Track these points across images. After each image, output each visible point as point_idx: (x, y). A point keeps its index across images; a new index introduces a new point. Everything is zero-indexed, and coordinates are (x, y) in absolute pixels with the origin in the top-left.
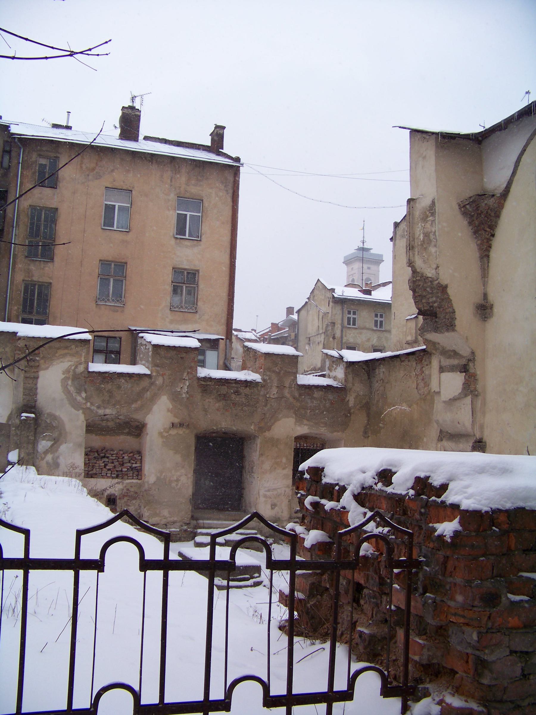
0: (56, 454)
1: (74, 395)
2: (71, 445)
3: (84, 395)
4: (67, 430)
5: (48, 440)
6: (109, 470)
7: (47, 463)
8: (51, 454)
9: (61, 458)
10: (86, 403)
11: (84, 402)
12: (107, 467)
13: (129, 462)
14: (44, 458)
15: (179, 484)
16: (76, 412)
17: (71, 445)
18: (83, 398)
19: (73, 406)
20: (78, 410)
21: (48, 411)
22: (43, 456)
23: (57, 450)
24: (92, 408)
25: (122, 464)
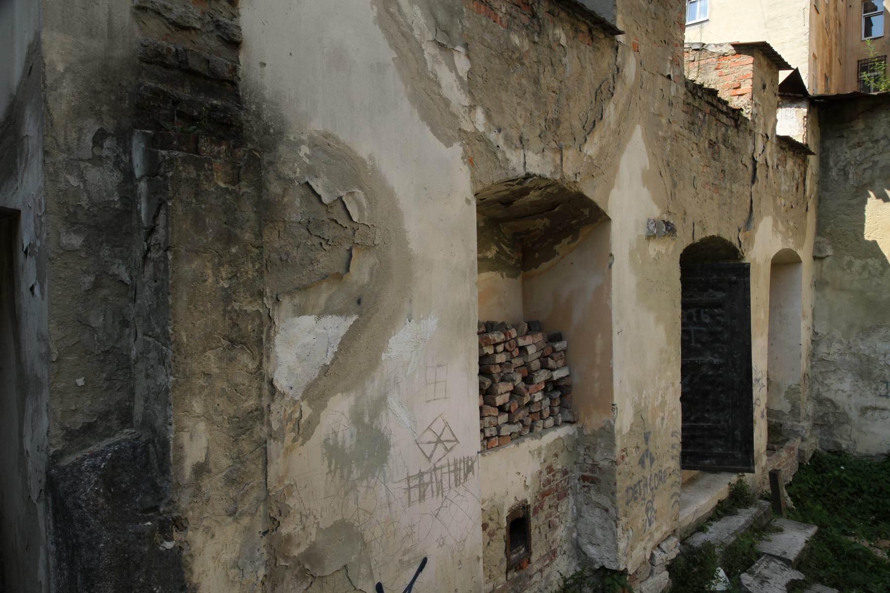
0: (372, 389)
1: (426, 56)
2: (431, 324)
3: (462, 64)
4: (414, 246)
5: (327, 311)
6: (501, 409)
7: (332, 451)
8: (346, 390)
9: (393, 401)
10: (472, 108)
11: (466, 101)
12: (499, 401)
13: (544, 366)
14: (312, 423)
15: (667, 414)
16: (439, 146)
17: (431, 324)
18: (460, 78)
19: (427, 117)
20: (448, 143)
21: (316, 126)
22: (307, 412)
23: (374, 362)
24: (493, 136)
25: (528, 380)
